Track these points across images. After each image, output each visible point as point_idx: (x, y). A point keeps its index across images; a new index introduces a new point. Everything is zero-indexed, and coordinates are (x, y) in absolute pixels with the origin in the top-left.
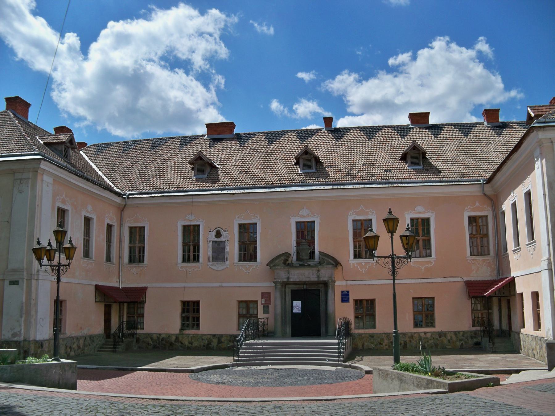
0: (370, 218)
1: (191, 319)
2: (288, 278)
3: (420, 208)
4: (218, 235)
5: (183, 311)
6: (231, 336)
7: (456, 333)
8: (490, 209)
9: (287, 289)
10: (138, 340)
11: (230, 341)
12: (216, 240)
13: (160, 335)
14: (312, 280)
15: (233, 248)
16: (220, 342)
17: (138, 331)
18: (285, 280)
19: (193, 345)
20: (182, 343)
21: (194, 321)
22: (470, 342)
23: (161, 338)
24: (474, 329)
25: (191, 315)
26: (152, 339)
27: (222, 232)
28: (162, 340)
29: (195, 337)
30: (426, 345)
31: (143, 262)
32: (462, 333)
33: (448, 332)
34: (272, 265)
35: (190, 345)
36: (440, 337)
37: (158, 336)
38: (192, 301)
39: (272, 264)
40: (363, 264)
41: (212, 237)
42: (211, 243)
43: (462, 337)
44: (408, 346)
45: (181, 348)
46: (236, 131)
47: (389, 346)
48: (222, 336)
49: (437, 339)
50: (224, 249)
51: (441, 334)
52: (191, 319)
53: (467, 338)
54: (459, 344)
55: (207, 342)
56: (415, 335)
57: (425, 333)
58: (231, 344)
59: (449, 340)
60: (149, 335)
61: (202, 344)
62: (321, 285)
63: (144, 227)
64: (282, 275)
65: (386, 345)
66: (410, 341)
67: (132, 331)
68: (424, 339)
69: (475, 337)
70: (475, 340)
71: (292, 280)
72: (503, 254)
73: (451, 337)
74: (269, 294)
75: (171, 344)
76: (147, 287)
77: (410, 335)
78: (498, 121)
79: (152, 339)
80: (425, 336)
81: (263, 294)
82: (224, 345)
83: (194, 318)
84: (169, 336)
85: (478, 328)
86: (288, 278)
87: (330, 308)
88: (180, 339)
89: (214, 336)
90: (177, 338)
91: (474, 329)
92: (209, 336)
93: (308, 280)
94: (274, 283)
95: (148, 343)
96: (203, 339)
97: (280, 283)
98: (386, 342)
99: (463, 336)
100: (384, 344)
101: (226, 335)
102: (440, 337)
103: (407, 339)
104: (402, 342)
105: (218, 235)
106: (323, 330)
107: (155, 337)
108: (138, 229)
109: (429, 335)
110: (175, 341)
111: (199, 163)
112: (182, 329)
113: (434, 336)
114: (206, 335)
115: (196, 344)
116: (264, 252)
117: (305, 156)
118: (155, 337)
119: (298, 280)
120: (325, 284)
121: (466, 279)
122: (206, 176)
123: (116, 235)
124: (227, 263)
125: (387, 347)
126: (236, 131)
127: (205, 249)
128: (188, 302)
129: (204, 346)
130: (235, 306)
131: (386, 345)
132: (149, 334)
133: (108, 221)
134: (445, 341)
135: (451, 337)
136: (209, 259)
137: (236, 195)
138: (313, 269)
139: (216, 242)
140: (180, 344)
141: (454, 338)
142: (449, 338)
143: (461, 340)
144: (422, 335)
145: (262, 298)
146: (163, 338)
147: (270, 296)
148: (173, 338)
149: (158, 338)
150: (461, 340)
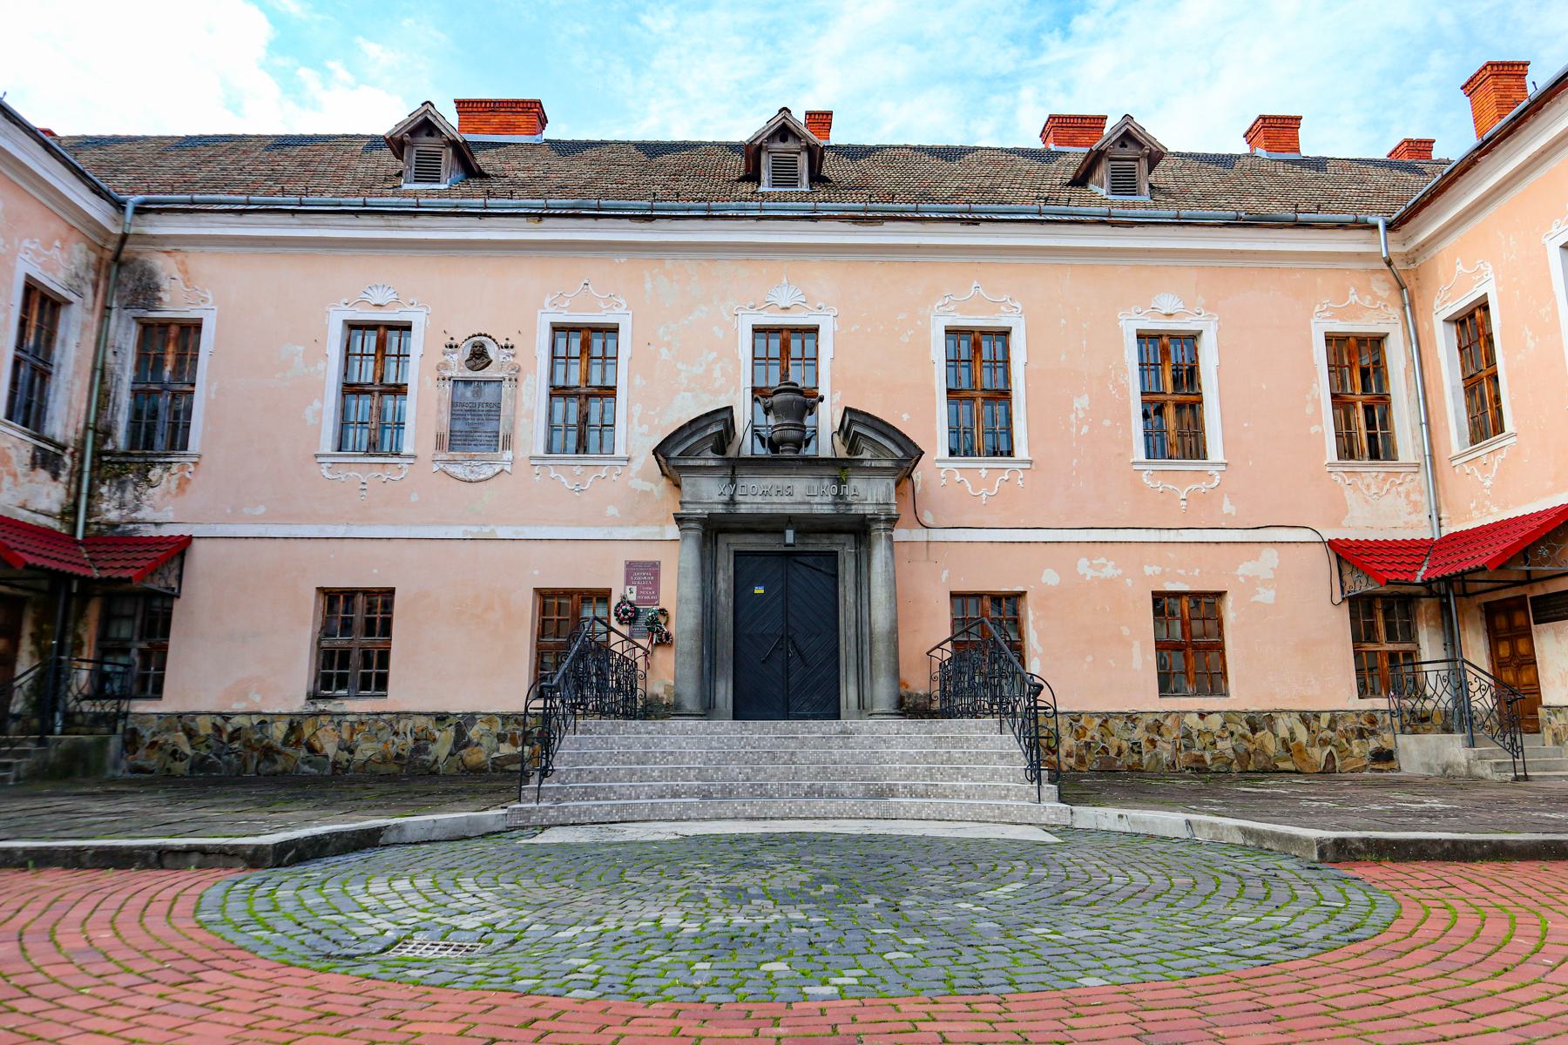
0: (1003, 323)
1: (356, 658)
2: (732, 501)
3: (1168, 302)
4: (479, 356)
5: (326, 631)
6: (505, 718)
7: (1306, 718)
8: (1395, 312)
9: (722, 546)
10: (132, 740)
11: (501, 738)
12: (469, 374)
13: (227, 717)
14: (818, 510)
15: (528, 408)
16: (461, 741)
17: (140, 707)
18: (719, 509)
19: (359, 756)
20: (311, 749)
21: (367, 663)
22: (1356, 751)
23: (230, 729)
24: (1367, 704)
25: (359, 640)
26: (191, 734)
27: (492, 351)
28: (236, 734)
29: (362, 722)
30: (1208, 757)
31: (185, 447)
32: (1325, 719)
33: (1281, 712)
34: (674, 454)
35: (346, 755)
36: (1254, 730)
37: (219, 721)
38: (367, 592)
39: (676, 453)
40: (984, 473)
41: (457, 365)
42: (448, 386)
43: (1330, 734)
44: (1146, 758)
45: (306, 768)
46: (550, 133)
47: (1081, 760)
48: (471, 718)
49: (1243, 737)
50: (495, 409)
51: (1257, 722)
52: (356, 658)
53: (1345, 734)
54: (1319, 755)
55: (410, 739)
56: (1169, 722)
57: (1202, 715)
58: (506, 749)
59: (1284, 741)
60: (183, 722)
61: (393, 750)
62: (842, 538)
63: (197, 326)
64: (709, 493)
65: (1069, 755)
66: (1153, 742)
67: (109, 707)
68: (1200, 733)
69: (1373, 733)
70: (1373, 743)
71: (743, 509)
72: (1456, 450)
73: (1292, 733)
74: (653, 568)
75: (269, 752)
76: (190, 538)
77: (1150, 719)
78: (1297, 150)
79: (191, 734)
80: (1201, 725)
81: (632, 568)
82: (473, 757)
83: (366, 656)
84: (263, 722)
85: (1381, 703)
86: (732, 501)
87: (880, 617)
88: (307, 731)
89: (441, 718)
90: (294, 728)
91: (1367, 704)
92: (421, 722)
93: (803, 510)
94: (680, 520)
95: (174, 752)
96: (396, 734)
97: (699, 520)
98: (1068, 742)
99: (1332, 726)
100: (1062, 752)
101: (490, 717)
102: (1254, 730)
103: (1139, 734)
104: (1125, 745)
105: (479, 356)
106: (849, 693)
107: (204, 727)
108: (174, 331)
109: (1215, 722)
110: (285, 742)
111: (426, 143)
112: (313, 697)
113: (1232, 727)
114: (408, 715)
115: (367, 750)
116: (640, 421)
117: (778, 146)
118: (204, 727)
119: (766, 510)
120: (860, 530)
121: (1329, 535)
122: (442, 187)
123: (72, 341)
124: (508, 455)
125: (1072, 761)
126: (550, 133)
127: (423, 411)
128: (350, 594)
129: (398, 756)
130: (526, 608)
131: (1069, 755)
132: (180, 716)
133: (27, 264)
134: (1272, 747)
135: (1292, 733)
136: (439, 446)
137: (547, 222)
138: (821, 471)
139: (468, 382)
140: (303, 753)
141: (1302, 735)
142: (1283, 732)
143: (1325, 742)
144: (1193, 721)
145: (628, 583)
146: (238, 730)
147: (656, 574)
148: (278, 731)
149: (218, 729)
150: (1325, 742)
